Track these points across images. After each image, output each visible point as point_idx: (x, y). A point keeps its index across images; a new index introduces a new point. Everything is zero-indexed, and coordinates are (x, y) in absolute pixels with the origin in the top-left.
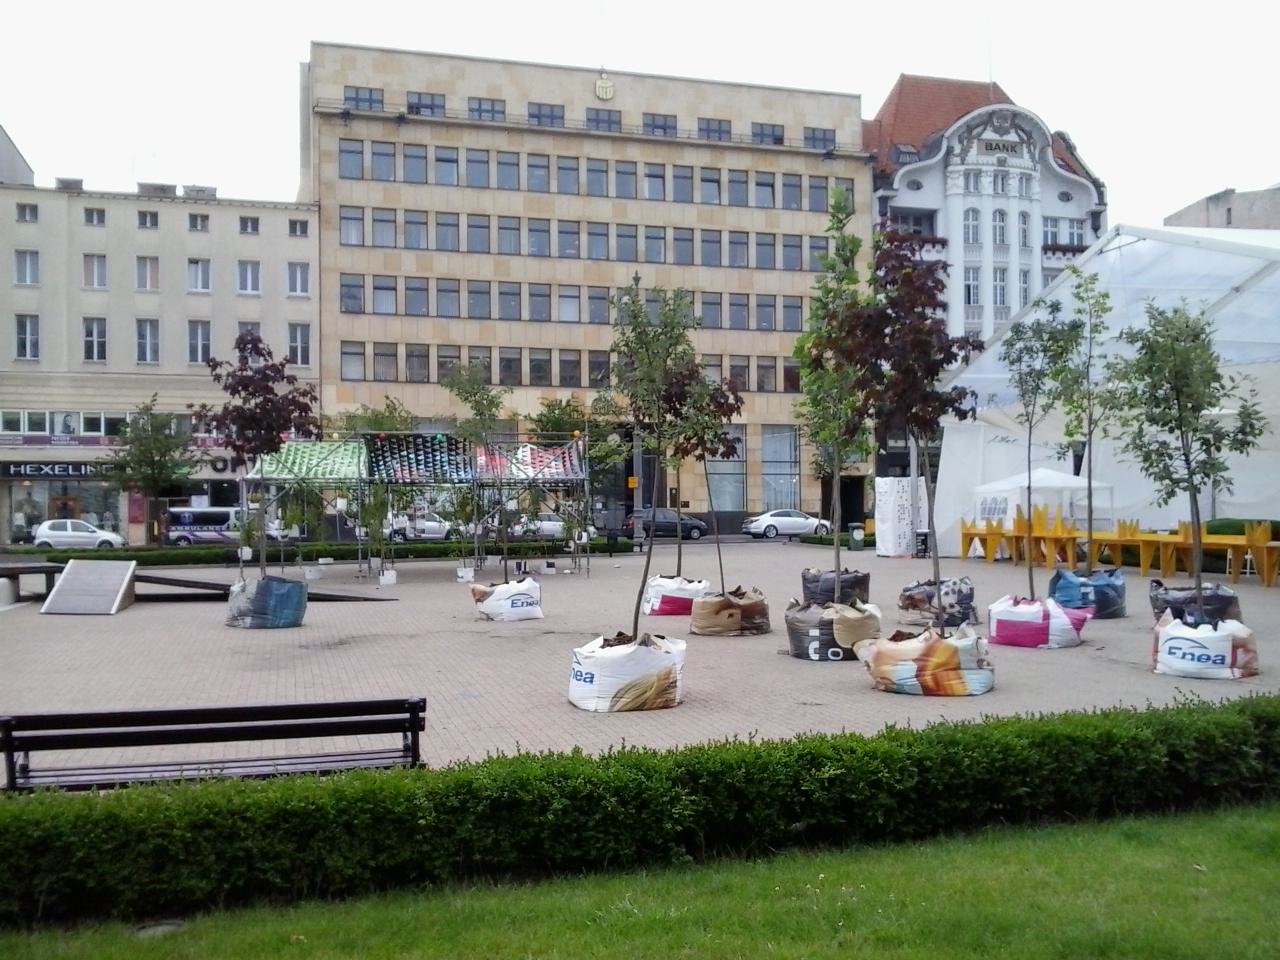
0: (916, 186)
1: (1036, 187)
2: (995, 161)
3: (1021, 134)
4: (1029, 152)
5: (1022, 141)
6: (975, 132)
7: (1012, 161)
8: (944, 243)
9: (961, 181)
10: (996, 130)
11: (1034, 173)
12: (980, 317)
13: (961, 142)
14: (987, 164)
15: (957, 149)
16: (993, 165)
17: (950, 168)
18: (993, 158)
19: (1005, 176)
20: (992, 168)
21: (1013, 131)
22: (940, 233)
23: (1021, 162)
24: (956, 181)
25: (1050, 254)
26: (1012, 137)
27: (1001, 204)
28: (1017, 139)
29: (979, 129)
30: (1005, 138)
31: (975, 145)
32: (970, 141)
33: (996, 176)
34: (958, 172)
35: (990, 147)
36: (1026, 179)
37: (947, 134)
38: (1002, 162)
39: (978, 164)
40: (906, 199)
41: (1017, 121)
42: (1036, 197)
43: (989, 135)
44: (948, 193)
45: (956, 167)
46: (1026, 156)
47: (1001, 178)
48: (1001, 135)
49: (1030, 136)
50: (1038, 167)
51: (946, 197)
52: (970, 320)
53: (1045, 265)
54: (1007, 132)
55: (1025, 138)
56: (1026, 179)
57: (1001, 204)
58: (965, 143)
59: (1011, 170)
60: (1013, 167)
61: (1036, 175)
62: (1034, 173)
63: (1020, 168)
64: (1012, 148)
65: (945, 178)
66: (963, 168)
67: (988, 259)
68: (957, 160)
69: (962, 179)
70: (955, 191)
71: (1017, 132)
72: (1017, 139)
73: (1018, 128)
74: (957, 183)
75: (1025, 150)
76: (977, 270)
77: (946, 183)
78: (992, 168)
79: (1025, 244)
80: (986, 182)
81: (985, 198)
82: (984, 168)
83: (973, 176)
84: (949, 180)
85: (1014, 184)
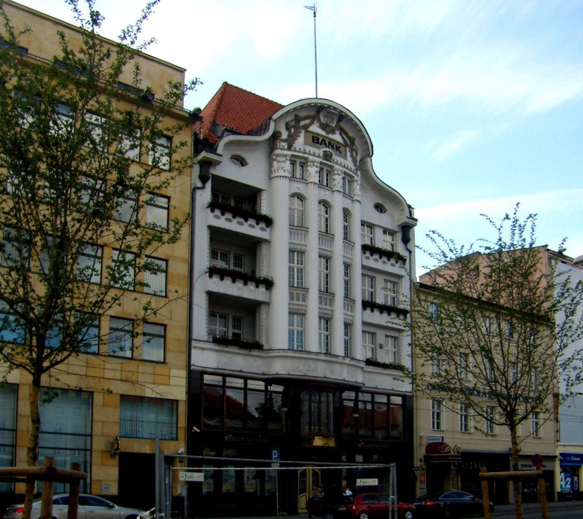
0: (242, 162)
1: (357, 188)
2: (321, 155)
4: (352, 156)
6: (302, 123)
7: (336, 158)
8: (268, 222)
9: (287, 165)
10: (323, 127)
12: (304, 300)
13: (288, 128)
14: (314, 155)
15: (285, 135)
16: (319, 157)
17: (278, 152)
18: (320, 151)
19: (330, 171)
20: (319, 160)
21: (338, 132)
22: (264, 210)
23: (344, 162)
24: (283, 165)
25: (368, 254)
26: (337, 137)
27: (326, 195)
28: (341, 141)
29: (307, 122)
30: (330, 136)
31: (302, 135)
32: (298, 129)
33: (321, 169)
34: (286, 156)
35: (316, 140)
36: (348, 179)
37: (275, 117)
38: (327, 156)
39: (305, 153)
41: (342, 124)
42: (356, 198)
43: (315, 128)
44: (274, 175)
45: (282, 150)
46: (349, 159)
47: (326, 171)
48: (328, 133)
49: (352, 141)
50: (359, 173)
51: (270, 178)
52: (295, 302)
53: (365, 264)
54: (333, 132)
57: (326, 195)
58: (293, 130)
59: (336, 166)
60: (337, 163)
61: (358, 178)
62: (356, 177)
63: (344, 167)
64: (337, 147)
65: (270, 160)
66: (290, 153)
67: (313, 245)
68: (285, 145)
69: (288, 162)
70: (281, 173)
71: (341, 134)
72: (341, 141)
73: (343, 132)
74: (283, 167)
75: (349, 154)
76: (302, 253)
77: (271, 166)
78: (319, 160)
79: (345, 238)
80: (313, 172)
81: (311, 186)
82: (311, 158)
83: (299, 163)
84: (275, 164)
85: (338, 180)
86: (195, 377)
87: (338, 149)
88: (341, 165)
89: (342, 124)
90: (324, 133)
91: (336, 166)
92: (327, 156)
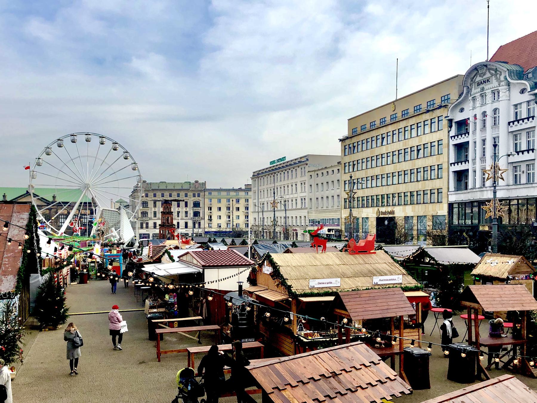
3: (491, 71)
4: (497, 79)
5: (492, 75)
10: (480, 76)
11: (499, 88)
30: (484, 77)
40: (459, 117)
43: (478, 79)
54: (485, 74)
55: (494, 72)
56: (496, 93)
59: (486, 91)
71: (489, 72)
73: (489, 69)
75: (494, 78)
86: (451, 206)
87: (488, 81)
88: (489, 89)
89: (489, 67)
90: (481, 78)
91: (486, 91)
92: (483, 89)
